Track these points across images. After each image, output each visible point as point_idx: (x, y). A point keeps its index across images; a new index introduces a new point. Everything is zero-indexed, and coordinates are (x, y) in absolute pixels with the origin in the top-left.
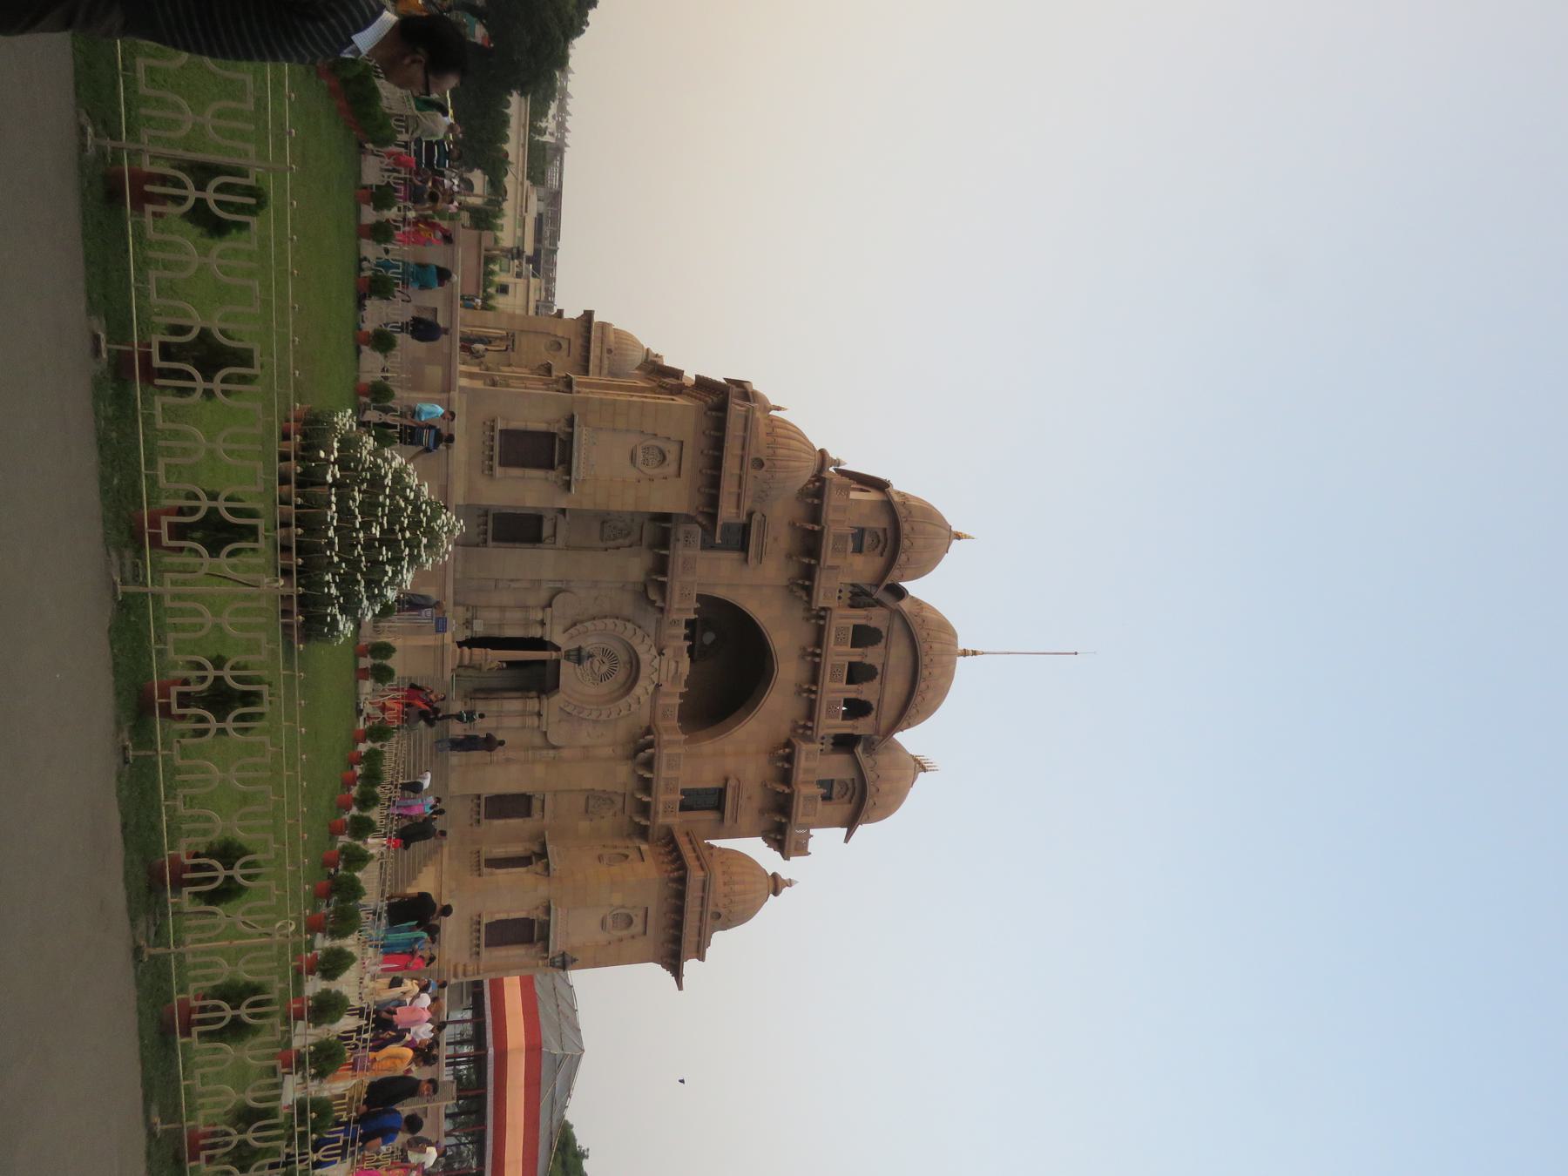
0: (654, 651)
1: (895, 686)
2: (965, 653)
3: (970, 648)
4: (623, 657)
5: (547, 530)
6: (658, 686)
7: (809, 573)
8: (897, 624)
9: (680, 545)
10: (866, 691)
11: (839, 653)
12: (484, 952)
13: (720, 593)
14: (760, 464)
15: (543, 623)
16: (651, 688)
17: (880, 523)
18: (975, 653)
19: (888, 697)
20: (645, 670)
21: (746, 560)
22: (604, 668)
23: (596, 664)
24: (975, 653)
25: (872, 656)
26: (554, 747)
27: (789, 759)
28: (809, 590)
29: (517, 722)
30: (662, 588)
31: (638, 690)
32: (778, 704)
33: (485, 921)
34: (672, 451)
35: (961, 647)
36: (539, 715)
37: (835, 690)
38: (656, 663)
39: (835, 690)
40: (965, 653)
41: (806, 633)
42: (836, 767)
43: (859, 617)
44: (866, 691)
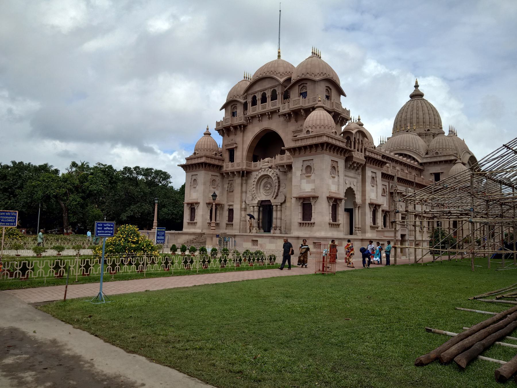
0: (260, 171)
1: (267, 84)
2: (279, 56)
3: (277, 54)
4: (265, 180)
5: (231, 208)
6: (270, 168)
7: (235, 127)
8: (250, 92)
9: (227, 169)
10: (269, 94)
11: (259, 108)
12: (312, 221)
13: (245, 153)
14: (195, 153)
15: (254, 207)
16: (270, 170)
17: (229, 108)
18: (279, 53)
19: (269, 86)
20: (265, 173)
21: (236, 147)
22: (269, 186)
23: (268, 188)
24: (279, 53)
25: (259, 97)
26: (285, 200)
27: (284, 115)
28: (240, 126)
29: (279, 213)
30: (239, 172)
31: (270, 175)
32: (275, 125)
33: (300, 221)
34: (194, 177)
35: (276, 58)
36: (277, 206)
37: (269, 106)
38: (263, 170)
39: (269, 106)
40: (279, 56)
41: (256, 121)
42: (294, 94)
43: (249, 105)
44: (269, 94)
